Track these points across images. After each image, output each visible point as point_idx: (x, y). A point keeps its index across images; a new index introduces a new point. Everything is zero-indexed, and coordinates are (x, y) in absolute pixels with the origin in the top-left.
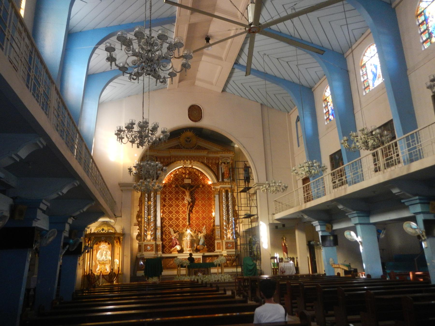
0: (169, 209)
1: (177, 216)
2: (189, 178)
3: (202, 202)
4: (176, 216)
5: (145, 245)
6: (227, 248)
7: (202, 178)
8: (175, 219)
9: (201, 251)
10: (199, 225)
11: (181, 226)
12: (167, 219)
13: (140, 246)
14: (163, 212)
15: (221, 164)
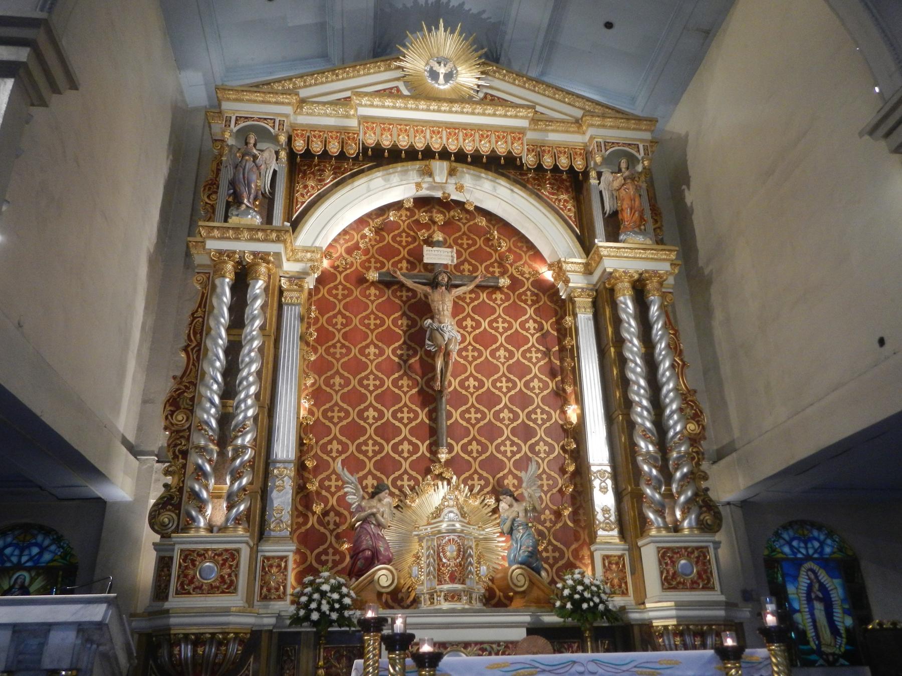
0: (348, 382)
1: (388, 415)
2: (450, 247)
3: (511, 355)
4: (381, 415)
5: (187, 555)
6: (670, 582)
7: (509, 250)
8: (376, 431)
9: (518, 602)
10: (502, 466)
11: (406, 465)
12: (336, 430)
13: (164, 564)
14: (318, 396)
15: (599, 175)
